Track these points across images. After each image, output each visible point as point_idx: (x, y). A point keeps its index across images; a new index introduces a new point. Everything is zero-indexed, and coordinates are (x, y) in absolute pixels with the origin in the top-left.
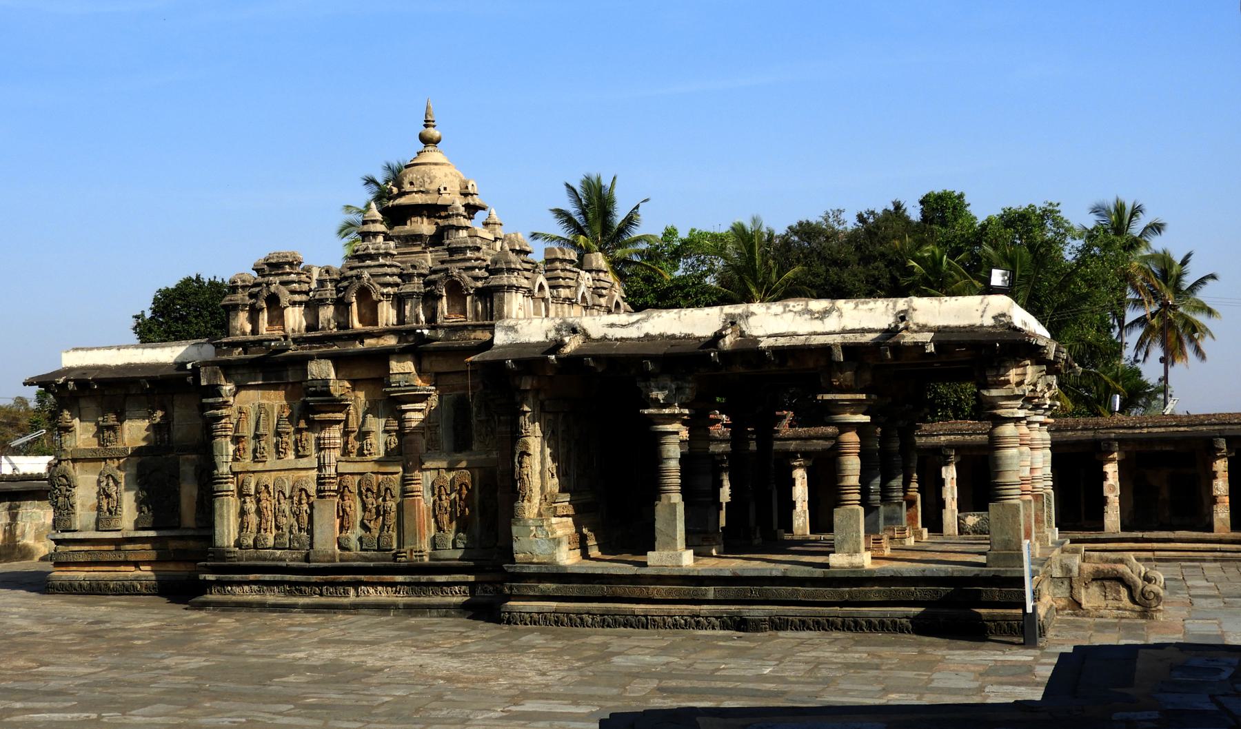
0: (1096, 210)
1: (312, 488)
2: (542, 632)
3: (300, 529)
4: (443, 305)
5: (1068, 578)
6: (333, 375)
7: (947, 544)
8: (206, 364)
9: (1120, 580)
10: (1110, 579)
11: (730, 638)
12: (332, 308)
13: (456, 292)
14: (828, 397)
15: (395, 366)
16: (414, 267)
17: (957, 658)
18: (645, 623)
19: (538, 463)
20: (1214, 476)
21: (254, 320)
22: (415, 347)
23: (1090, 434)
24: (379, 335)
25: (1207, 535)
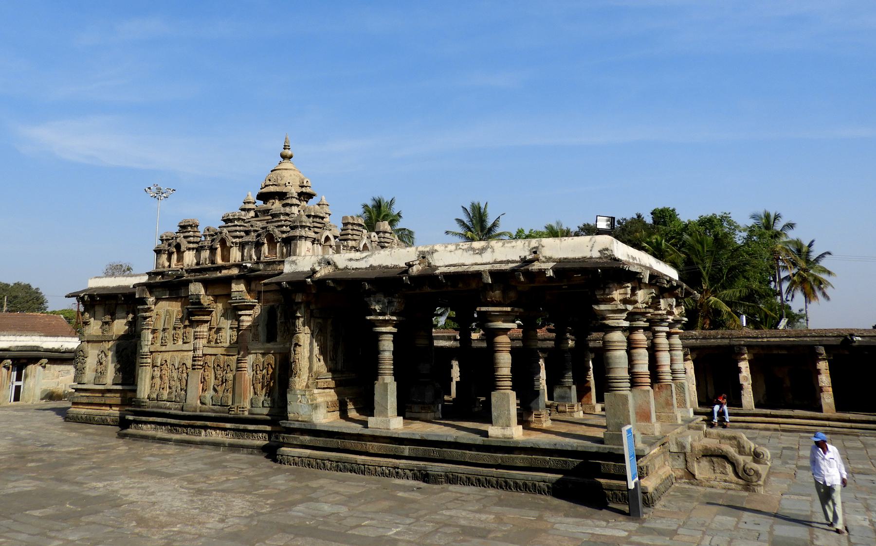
0: (753, 217)
1: (189, 363)
2: (292, 472)
3: (181, 390)
4: (265, 249)
5: (682, 452)
6: (203, 292)
7: (568, 423)
8: (139, 285)
9: (725, 457)
10: (717, 456)
11: (410, 489)
12: (208, 252)
13: (271, 239)
14: (484, 309)
15: (235, 287)
16: (252, 226)
17: (562, 528)
18: (361, 470)
19: (307, 351)
20: (818, 372)
21: (169, 259)
22: (249, 277)
23: (726, 341)
24: (229, 268)
25: (818, 414)
